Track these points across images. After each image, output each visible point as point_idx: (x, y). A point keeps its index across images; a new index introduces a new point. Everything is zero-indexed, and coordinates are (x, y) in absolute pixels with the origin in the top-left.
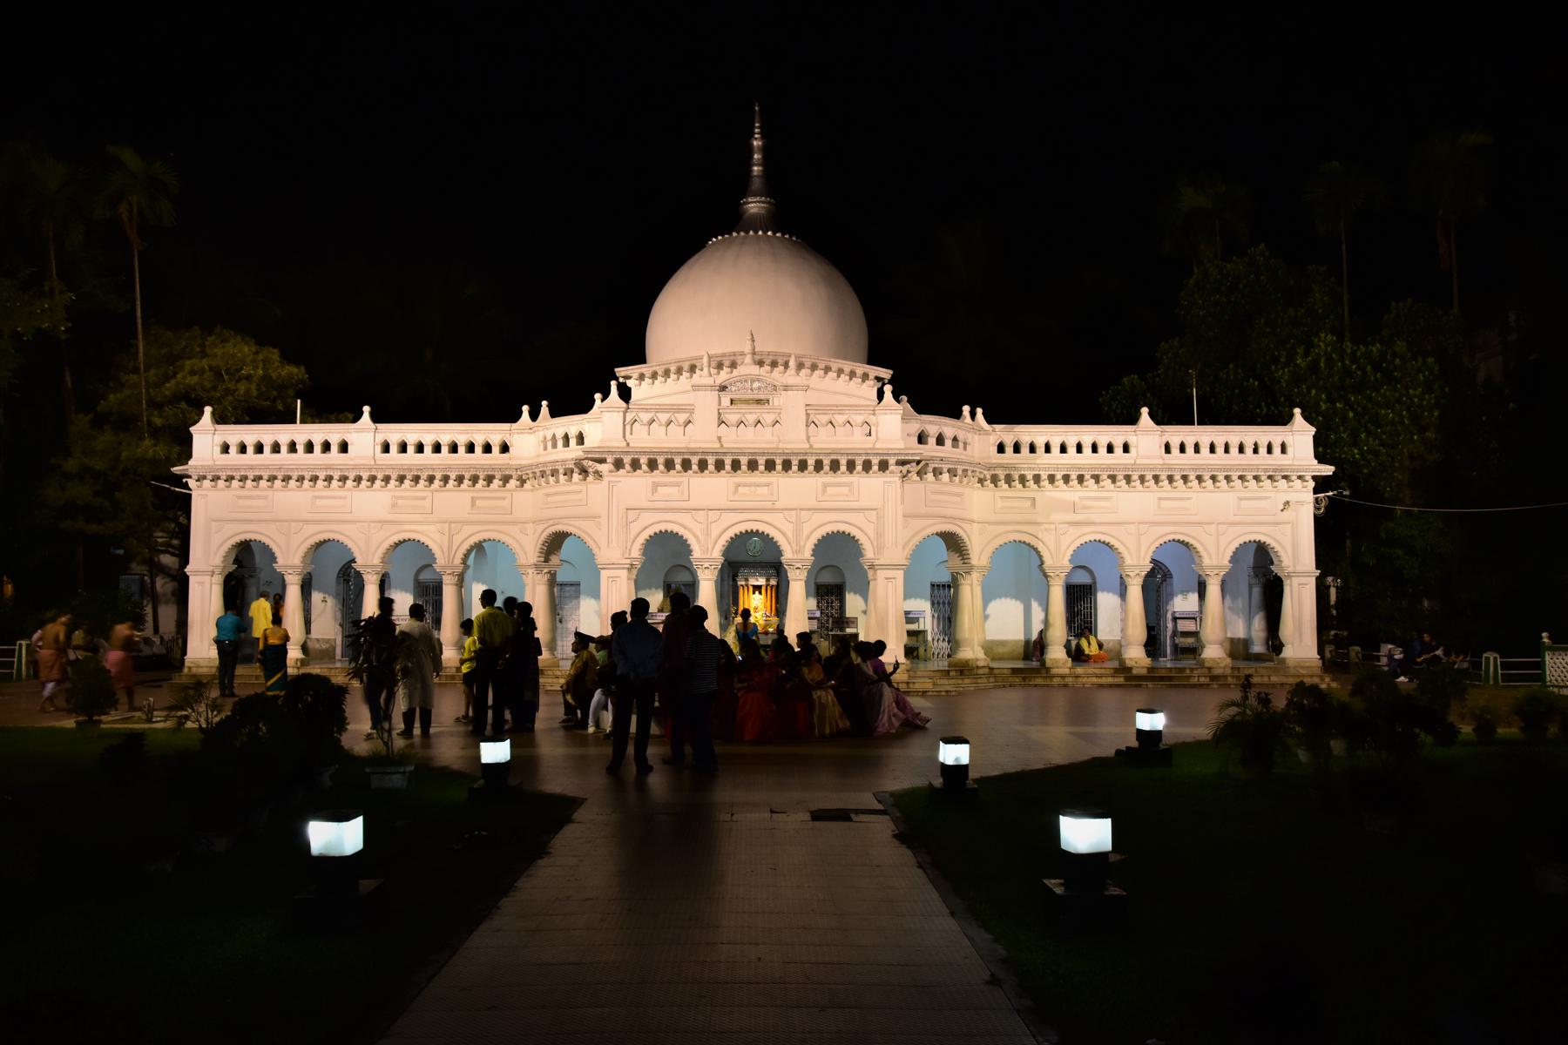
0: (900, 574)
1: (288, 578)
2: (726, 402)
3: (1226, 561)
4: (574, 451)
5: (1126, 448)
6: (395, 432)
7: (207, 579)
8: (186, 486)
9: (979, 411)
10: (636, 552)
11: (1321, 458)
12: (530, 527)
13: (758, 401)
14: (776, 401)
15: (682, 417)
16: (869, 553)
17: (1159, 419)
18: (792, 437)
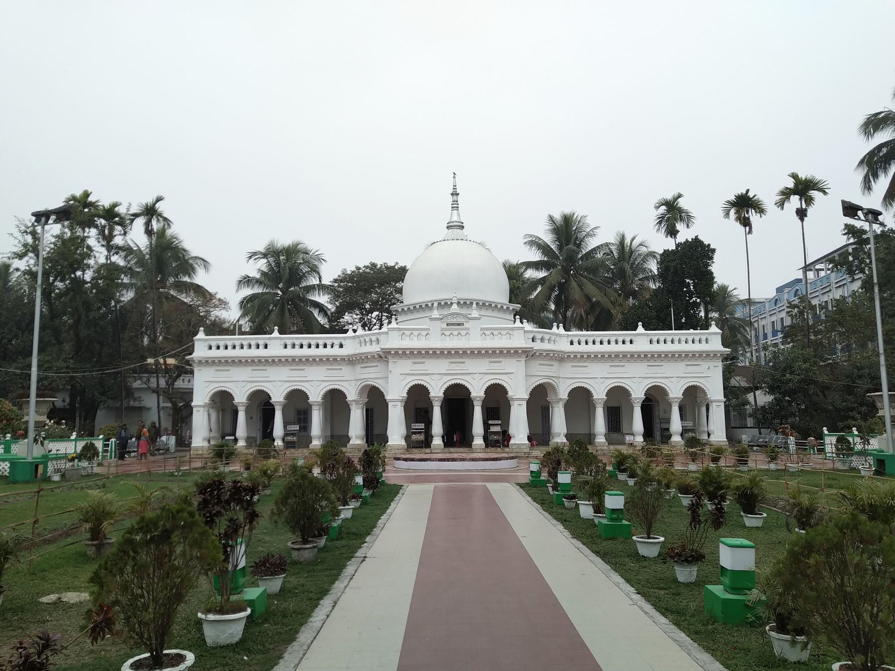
0: (524, 403)
1: (240, 408)
2: (445, 326)
3: (681, 396)
4: (375, 348)
5: (631, 342)
6: (290, 338)
7: (202, 409)
8: (190, 365)
9: (561, 325)
10: (405, 395)
11: (725, 344)
12: (353, 383)
13: (459, 325)
14: (466, 325)
15: (426, 332)
16: (510, 394)
17: (646, 328)
18: (476, 342)
